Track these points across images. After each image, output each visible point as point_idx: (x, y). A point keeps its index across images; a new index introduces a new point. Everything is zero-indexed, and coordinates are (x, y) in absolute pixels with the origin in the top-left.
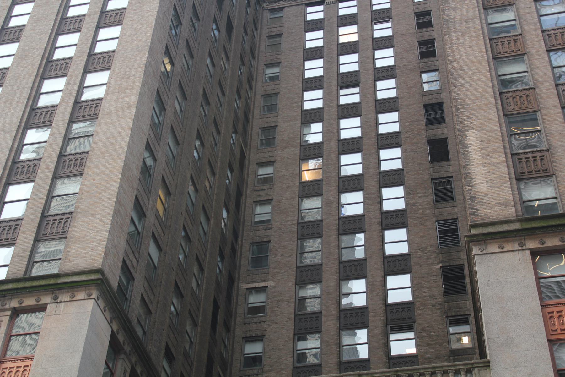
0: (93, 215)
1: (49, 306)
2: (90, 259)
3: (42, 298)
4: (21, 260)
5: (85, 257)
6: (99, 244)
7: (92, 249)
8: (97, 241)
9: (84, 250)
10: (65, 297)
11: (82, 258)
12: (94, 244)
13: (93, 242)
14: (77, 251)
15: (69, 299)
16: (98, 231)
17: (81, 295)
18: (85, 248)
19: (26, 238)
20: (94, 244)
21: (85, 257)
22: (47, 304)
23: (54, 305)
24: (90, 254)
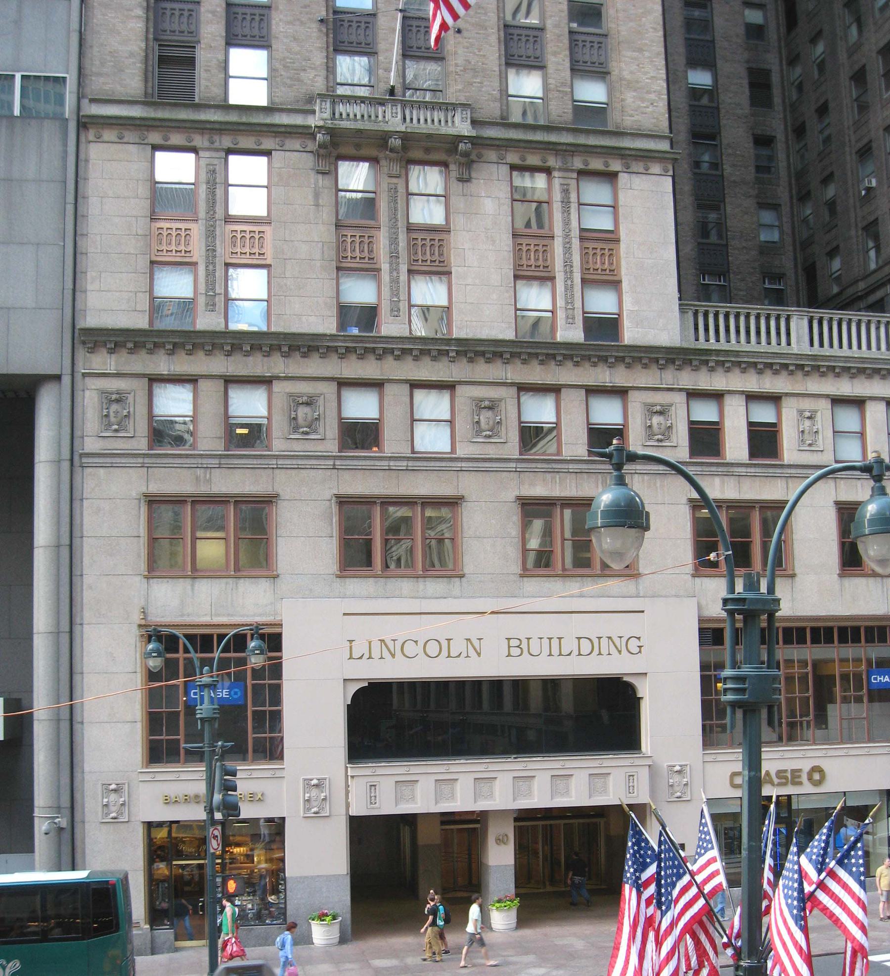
0: (640, 50)
1: (620, 175)
2: (654, 118)
3: (611, 161)
4: (562, 98)
5: (646, 113)
6: (659, 98)
7: (652, 104)
8: (654, 92)
9: (643, 102)
10: (638, 166)
11: (643, 113)
12: (653, 96)
13: (649, 92)
14: (634, 102)
15: (642, 170)
16: (652, 77)
17: (656, 168)
18: (643, 100)
19: (559, 64)
20: (653, 96)
21: (646, 113)
22: (618, 172)
23: (625, 175)
24: (650, 109)
